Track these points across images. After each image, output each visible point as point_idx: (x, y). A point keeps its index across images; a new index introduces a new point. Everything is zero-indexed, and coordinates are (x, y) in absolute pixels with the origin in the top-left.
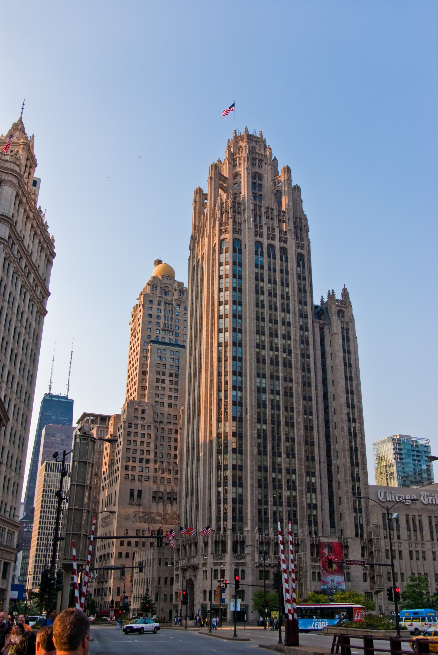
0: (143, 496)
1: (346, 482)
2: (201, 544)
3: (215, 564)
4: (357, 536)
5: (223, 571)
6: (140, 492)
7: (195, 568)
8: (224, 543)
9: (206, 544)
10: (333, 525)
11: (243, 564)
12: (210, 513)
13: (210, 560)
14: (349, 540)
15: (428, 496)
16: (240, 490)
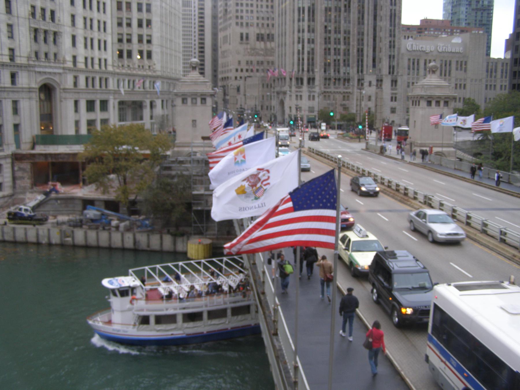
0: (250, 37)
1: (386, 38)
2: (288, 79)
3: (297, 91)
4: (390, 73)
5: (301, 96)
6: (247, 34)
7: (285, 93)
8: (302, 80)
9: (291, 79)
10: (374, 66)
11: (314, 92)
12: (293, 59)
13: (294, 89)
14: (384, 76)
15: (443, 46)
16: (312, 46)
